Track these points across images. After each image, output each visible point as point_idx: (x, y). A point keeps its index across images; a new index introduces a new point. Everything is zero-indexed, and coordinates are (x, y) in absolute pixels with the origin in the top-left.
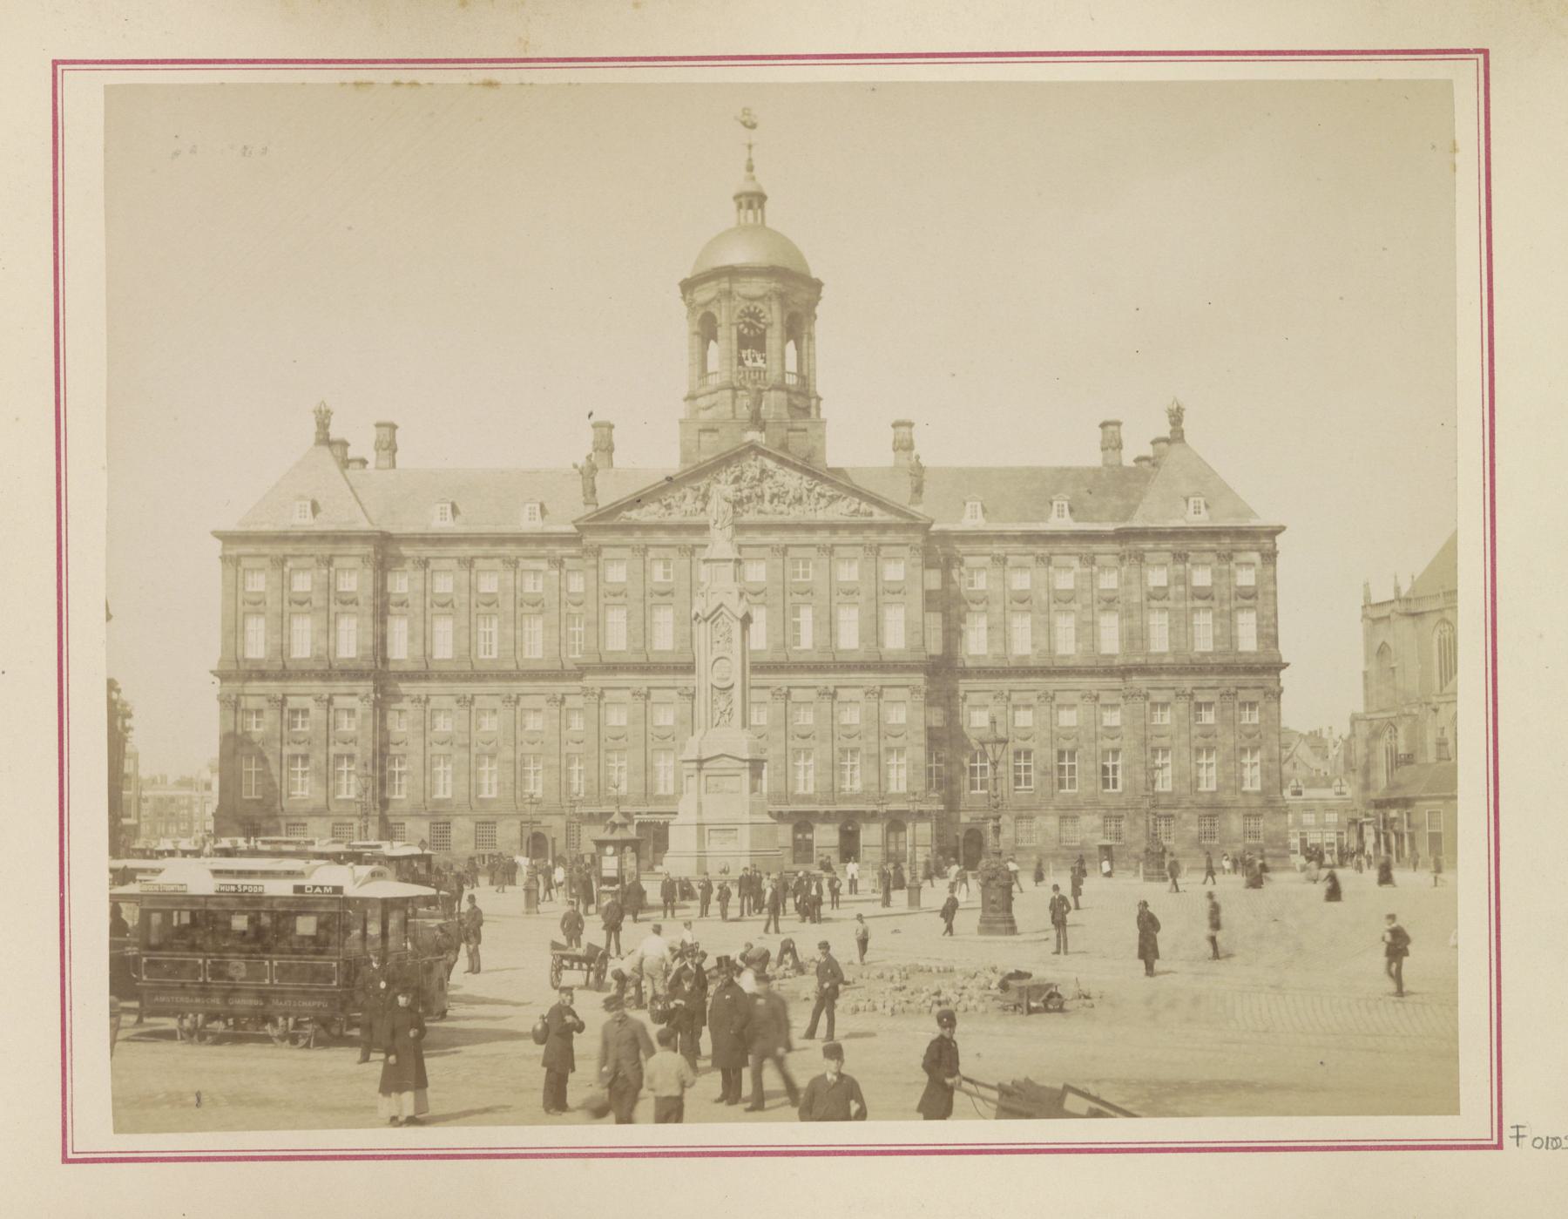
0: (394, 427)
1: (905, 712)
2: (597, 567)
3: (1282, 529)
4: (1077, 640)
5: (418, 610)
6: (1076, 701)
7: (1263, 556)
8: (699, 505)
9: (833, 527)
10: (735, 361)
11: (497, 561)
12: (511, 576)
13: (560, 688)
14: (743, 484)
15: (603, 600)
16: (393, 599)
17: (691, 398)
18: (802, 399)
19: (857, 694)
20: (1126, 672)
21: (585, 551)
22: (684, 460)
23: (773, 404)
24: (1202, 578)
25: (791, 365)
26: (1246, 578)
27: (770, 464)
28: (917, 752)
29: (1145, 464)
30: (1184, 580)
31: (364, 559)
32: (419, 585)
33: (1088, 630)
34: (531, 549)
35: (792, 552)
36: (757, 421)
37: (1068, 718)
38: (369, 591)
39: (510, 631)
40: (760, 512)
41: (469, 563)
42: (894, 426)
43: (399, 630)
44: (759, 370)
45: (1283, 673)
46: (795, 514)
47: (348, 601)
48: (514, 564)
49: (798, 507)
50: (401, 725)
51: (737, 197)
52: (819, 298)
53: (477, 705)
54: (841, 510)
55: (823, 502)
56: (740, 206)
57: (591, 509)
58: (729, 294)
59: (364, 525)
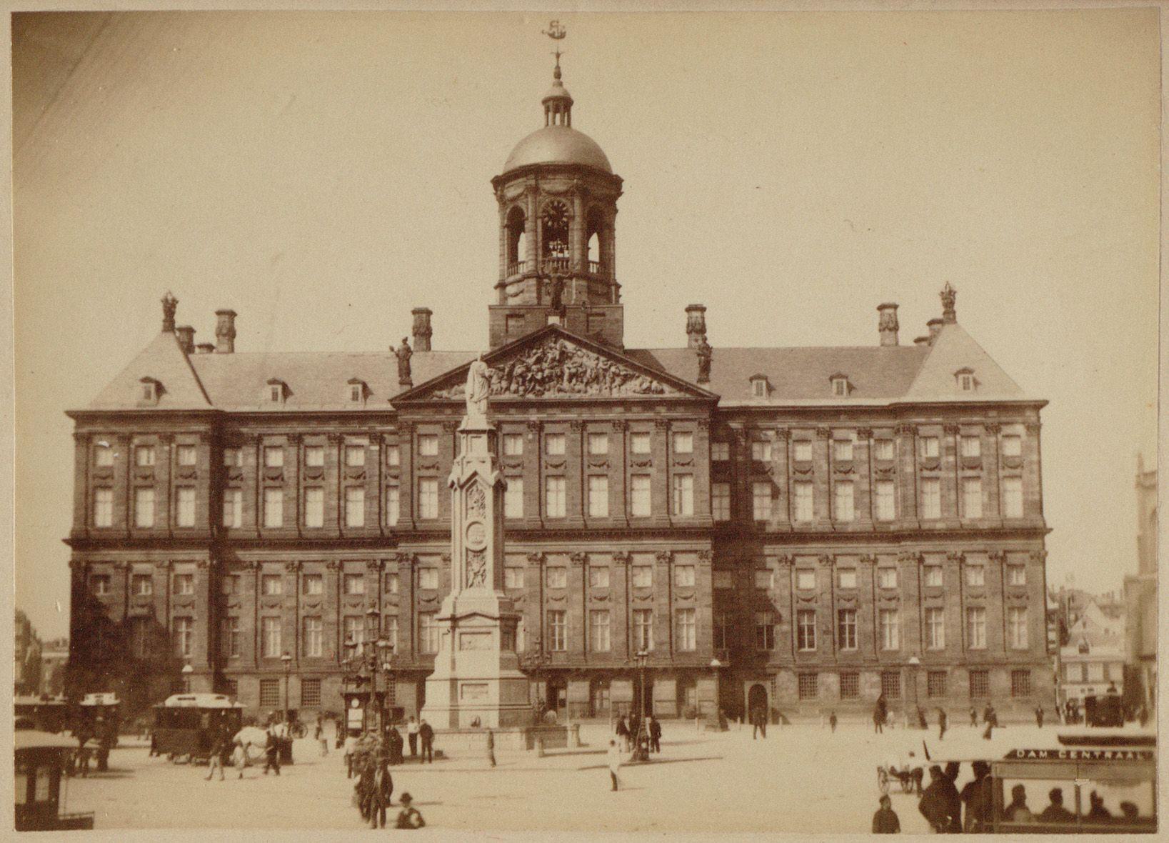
0: (232, 314)
1: (694, 576)
2: (412, 441)
3: (1045, 403)
4: (856, 508)
5: (252, 483)
6: (855, 564)
8: (504, 384)
9: (625, 404)
10: (540, 252)
11: (322, 437)
12: (335, 451)
13: (381, 554)
14: (545, 365)
15: (417, 473)
16: (232, 473)
17: (502, 286)
18: (603, 284)
19: (651, 558)
20: (897, 537)
21: (400, 428)
22: (493, 344)
23: (574, 292)
24: (972, 449)
25: (594, 255)
27: (570, 346)
28: (705, 613)
29: (924, 344)
30: (954, 450)
31: (204, 437)
32: (252, 461)
33: (867, 501)
34: (355, 427)
35: (591, 428)
36: (558, 307)
37: (848, 581)
38: (206, 465)
39: (334, 503)
40: (560, 390)
41: (297, 439)
42: (689, 309)
44: (563, 260)
45: (1048, 538)
46: (593, 392)
47: (191, 474)
48: (338, 440)
49: (595, 386)
50: (241, 591)
51: (545, 102)
52: (620, 194)
53: (305, 571)
54: (632, 389)
55: (618, 381)
56: (547, 111)
57: (407, 388)
58: (536, 190)
59: (202, 405)
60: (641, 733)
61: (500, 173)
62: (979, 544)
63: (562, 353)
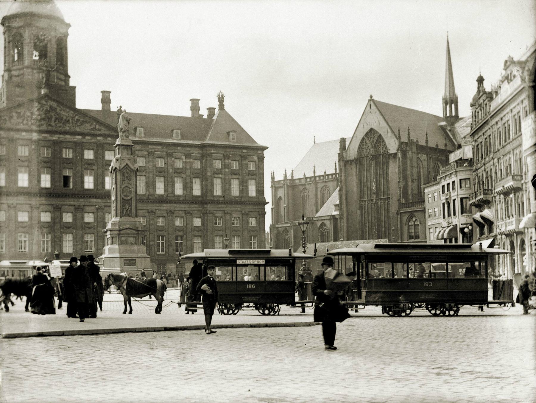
7: (259, 158)
9: (83, 135)
26: (252, 167)
27: (54, 104)
40: (50, 125)
60: (330, 316)
62: (239, 207)
63: (51, 107)
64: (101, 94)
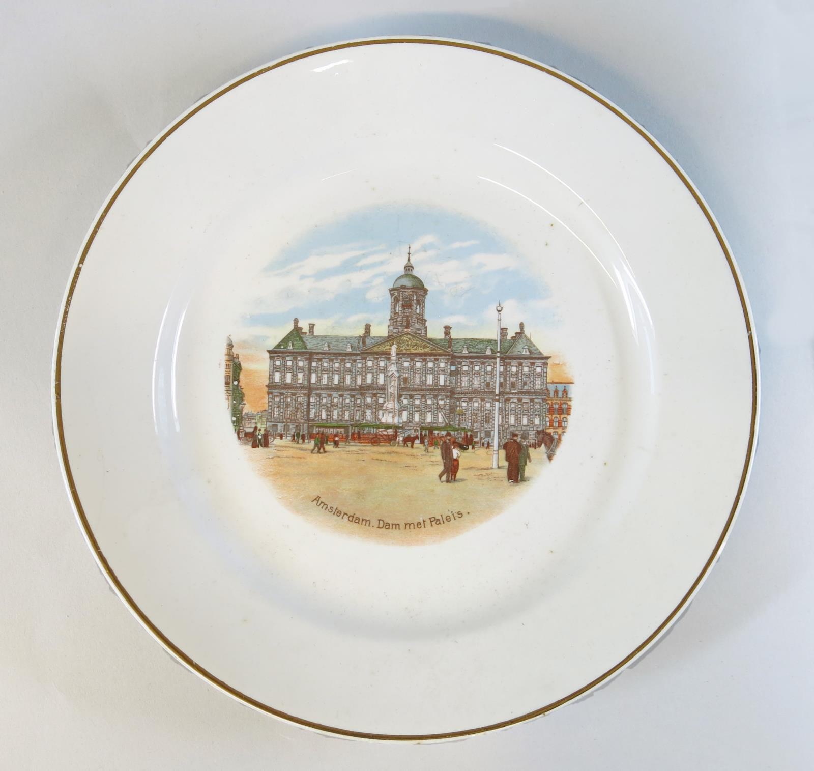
0: (314, 325)
43: (314, 376)
47: (302, 369)
52: (426, 294)
61: (391, 286)
64: (444, 329)
